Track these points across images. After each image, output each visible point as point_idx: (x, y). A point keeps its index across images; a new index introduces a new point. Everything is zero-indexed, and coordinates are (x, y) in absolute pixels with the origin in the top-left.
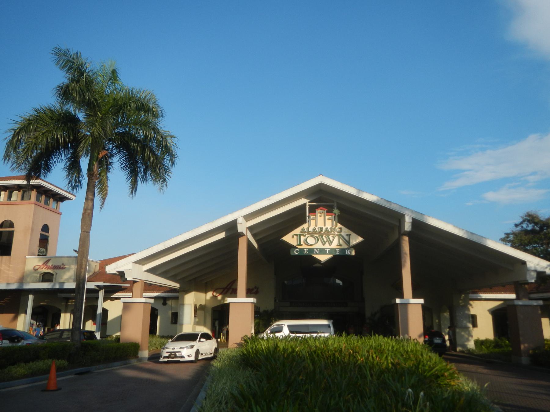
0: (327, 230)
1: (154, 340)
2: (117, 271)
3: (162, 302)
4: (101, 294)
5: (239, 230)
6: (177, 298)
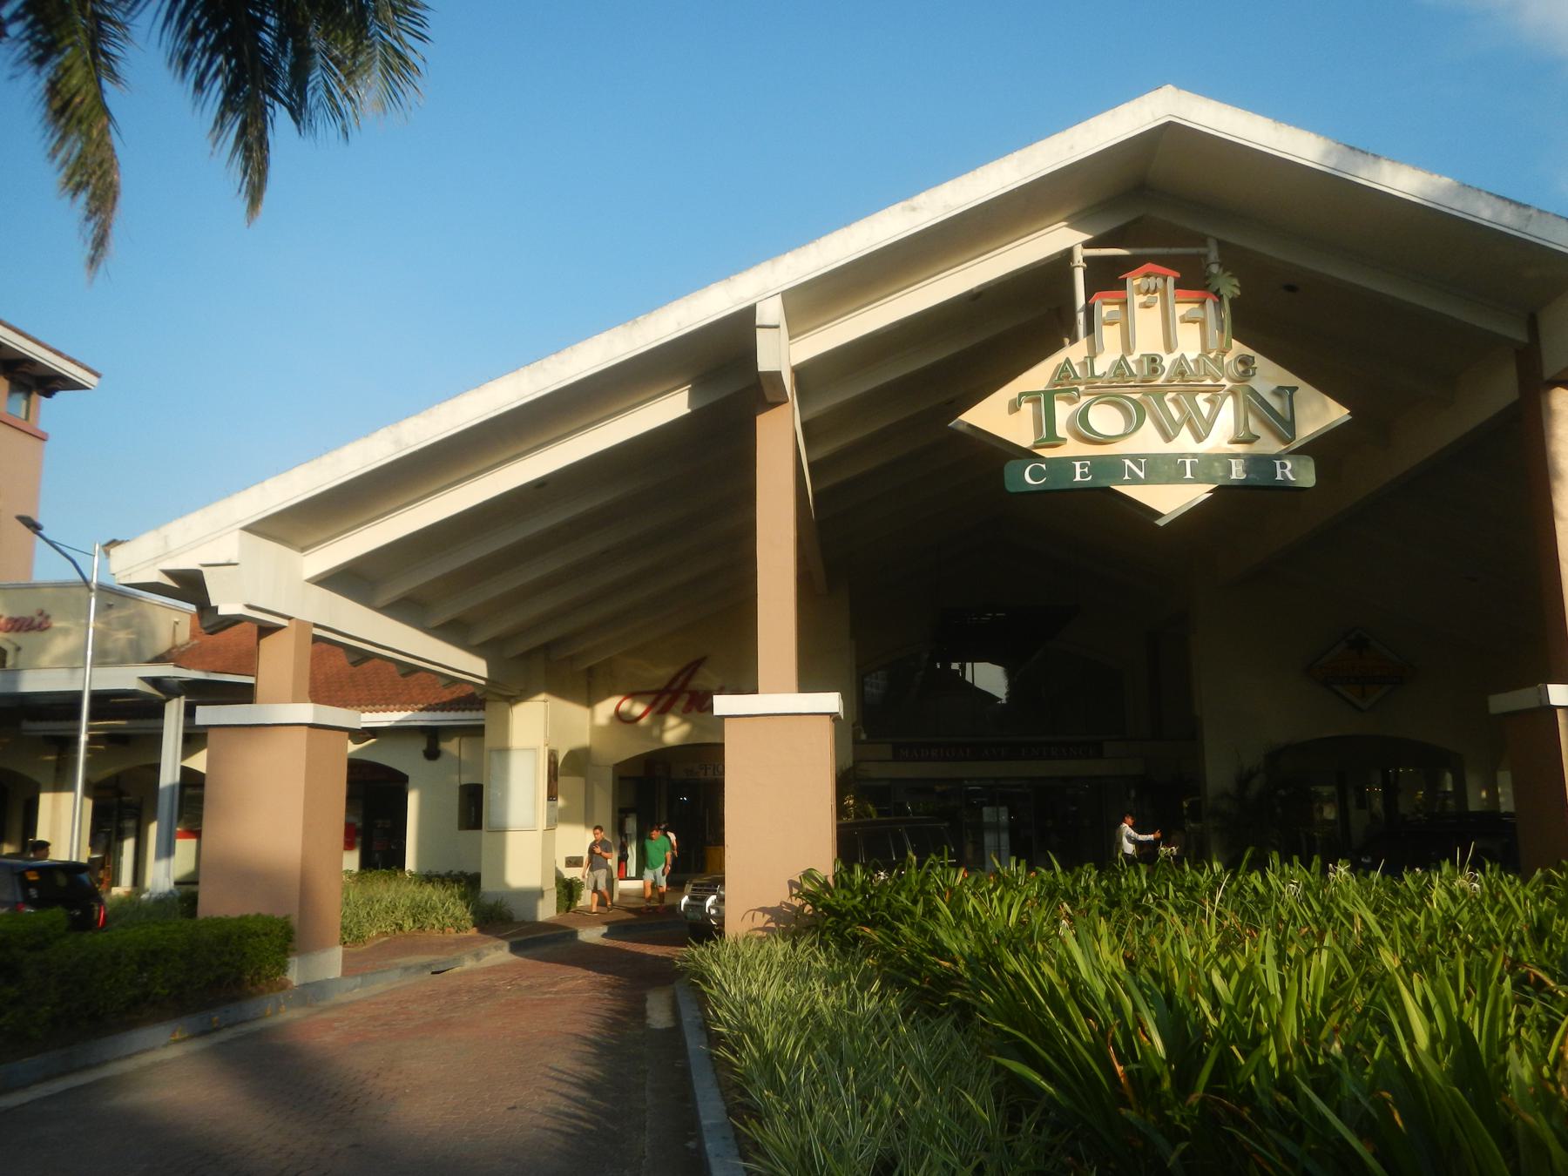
0: (1181, 370)
1: (384, 890)
2: (168, 573)
3: (424, 746)
4: (174, 712)
5: (765, 363)
6: (477, 731)
